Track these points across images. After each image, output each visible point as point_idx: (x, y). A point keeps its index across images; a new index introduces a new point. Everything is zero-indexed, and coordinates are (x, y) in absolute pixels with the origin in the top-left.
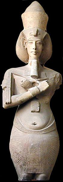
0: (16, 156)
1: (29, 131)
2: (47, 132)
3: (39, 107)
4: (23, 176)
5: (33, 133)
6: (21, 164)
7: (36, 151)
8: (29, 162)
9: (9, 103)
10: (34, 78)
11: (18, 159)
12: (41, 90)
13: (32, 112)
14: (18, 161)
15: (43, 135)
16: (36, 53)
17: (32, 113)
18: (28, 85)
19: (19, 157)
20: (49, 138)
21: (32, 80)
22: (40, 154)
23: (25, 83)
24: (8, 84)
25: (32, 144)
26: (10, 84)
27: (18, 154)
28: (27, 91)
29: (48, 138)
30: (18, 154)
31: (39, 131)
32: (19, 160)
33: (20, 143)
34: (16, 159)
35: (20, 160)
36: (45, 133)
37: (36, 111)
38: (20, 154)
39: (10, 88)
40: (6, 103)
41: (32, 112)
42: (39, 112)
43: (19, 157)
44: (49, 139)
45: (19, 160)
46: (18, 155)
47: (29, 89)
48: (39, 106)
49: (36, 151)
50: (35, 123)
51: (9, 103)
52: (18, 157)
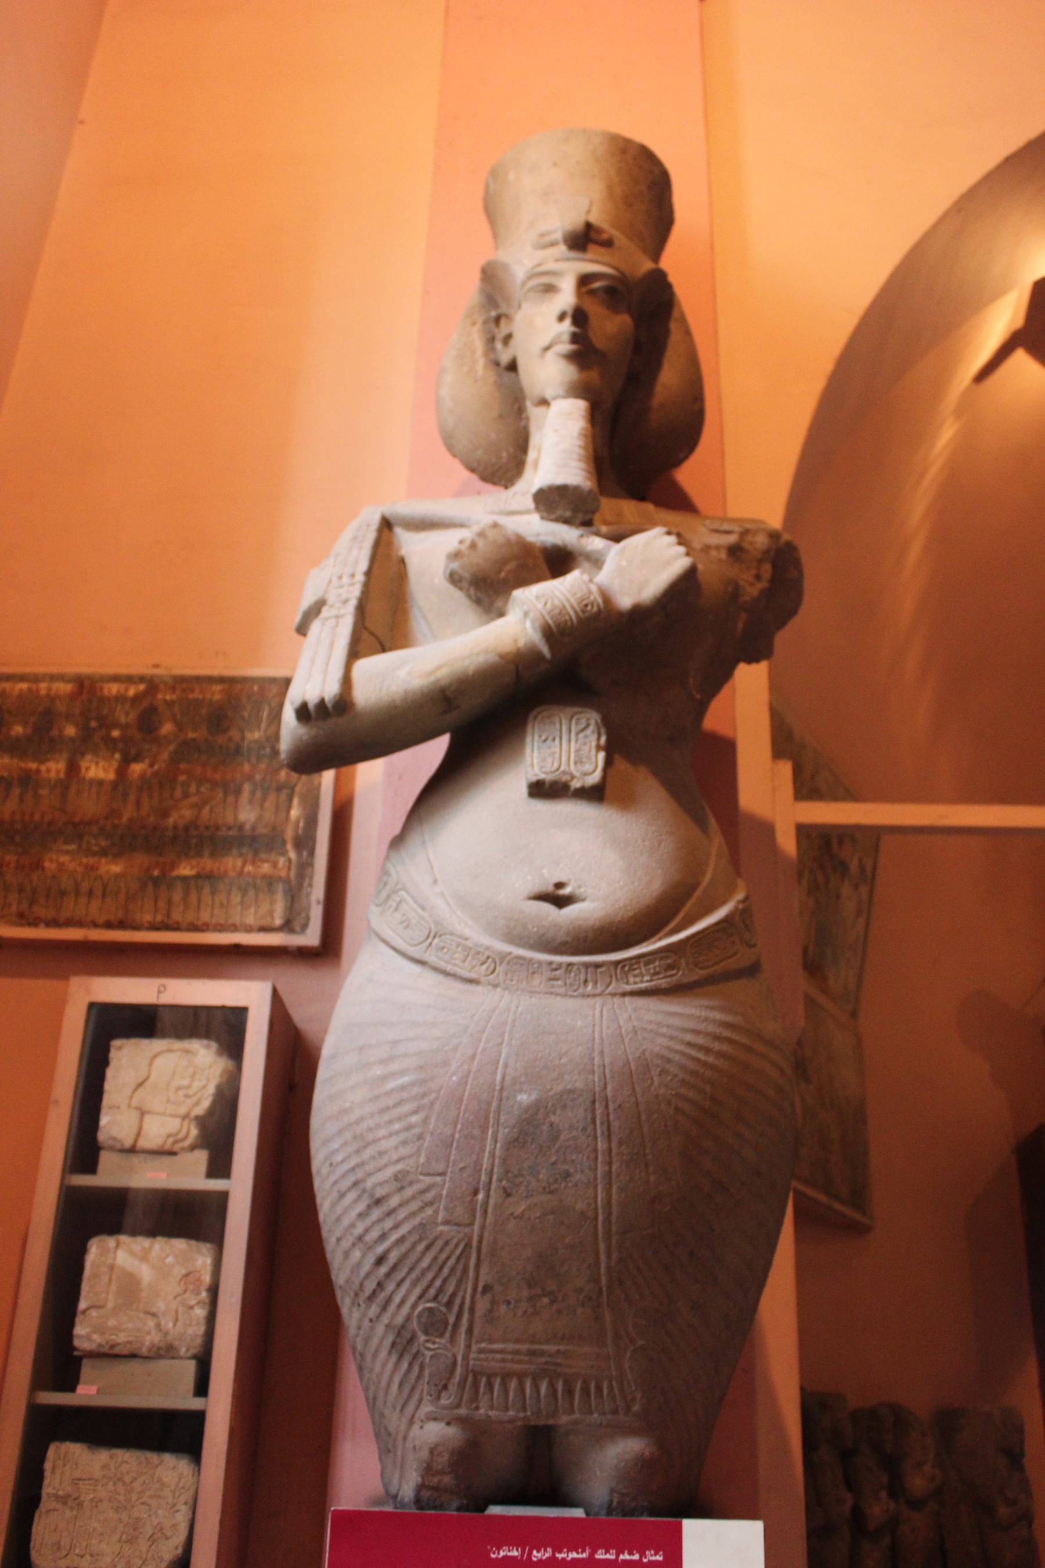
0: (359, 1230)
1: (503, 957)
2: (679, 976)
3: (602, 755)
4: (425, 1454)
5: (537, 980)
6: (399, 1320)
7: (567, 1175)
8: (487, 1289)
9: (322, 701)
10: (567, 521)
11: (380, 1261)
12: (625, 601)
13: (540, 790)
14: (370, 1286)
15: (641, 1002)
16: (583, 351)
17: (543, 807)
18: (511, 566)
19: (383, 1237)
20: (700, 1040)
21: (543, 531)
22: (608, 1203)
23: (481, 543)
24: (346, 580)
25: (523, 1098)
26: (360, 578)
27: (378, 1202)
28: (501, 614)
29: (688, 1037)
30: (378, 1202)
31: (597, 966)
32: (383, 1270)
33: (403, 1088)
34: (357, 1254)
35: (394, 1268)
36: (662, 982)
37: (576, 784)
38: (394, 1201)
39: (353, 603)
40: (303, 713)
41: (540, 790)
42: (595, 794)
43: (383, 1237)
44: (707, 1051)
45: (383, 1270)
46: (376, 1213)
47: (519, 594)
48: (599, 748)
49: (567, 1175)
50: (566, 891)
51: (322, 701)
52: (375, 1234)
